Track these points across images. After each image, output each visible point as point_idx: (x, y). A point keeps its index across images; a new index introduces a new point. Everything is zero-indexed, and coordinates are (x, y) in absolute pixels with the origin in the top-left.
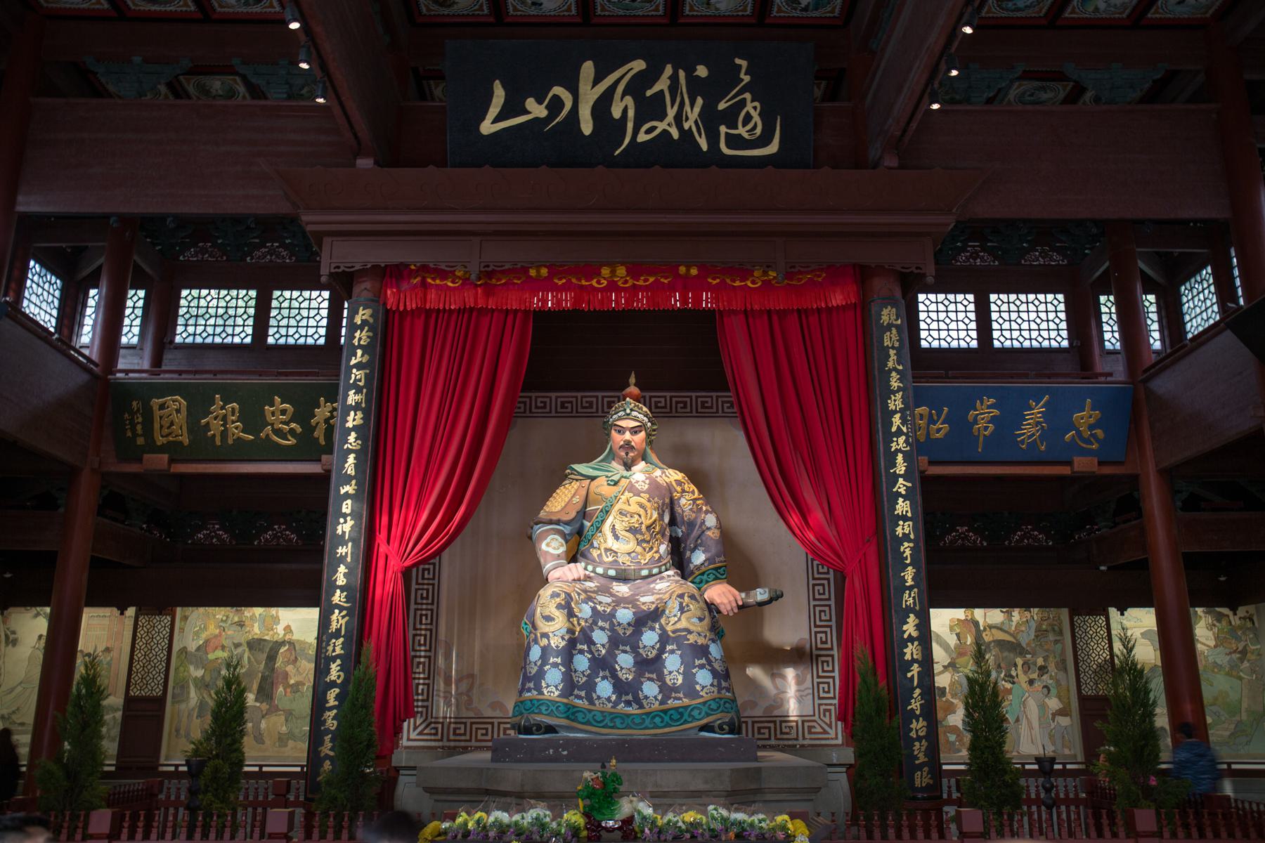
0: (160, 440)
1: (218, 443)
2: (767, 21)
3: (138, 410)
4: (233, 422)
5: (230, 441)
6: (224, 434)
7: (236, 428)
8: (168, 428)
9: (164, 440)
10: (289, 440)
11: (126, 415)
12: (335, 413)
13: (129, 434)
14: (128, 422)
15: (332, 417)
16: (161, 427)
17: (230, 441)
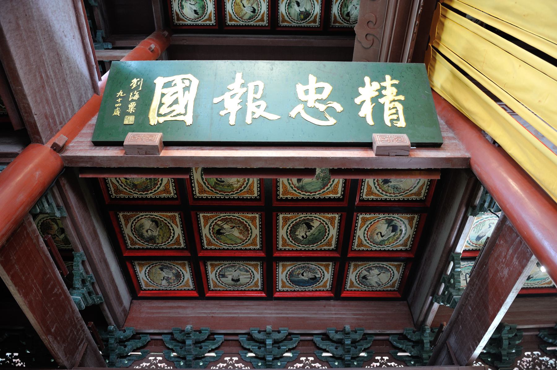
0: (153, 120)
1: (232, 121)
2: (344, 295)
3: (138, 86)
4: (255, 100)
5: (249, 120)
6: (242, 112)
7: (258, 106)
8: (170, 106)
9: (161, 120)
10: (327, 120)
11: (121, 93)
12: (384, 92)
13: (117, 113)
14: (119, 100)
15: (381, 96)
16: (161, 104)
17: (249, 120)
